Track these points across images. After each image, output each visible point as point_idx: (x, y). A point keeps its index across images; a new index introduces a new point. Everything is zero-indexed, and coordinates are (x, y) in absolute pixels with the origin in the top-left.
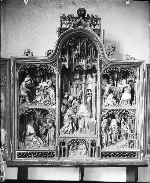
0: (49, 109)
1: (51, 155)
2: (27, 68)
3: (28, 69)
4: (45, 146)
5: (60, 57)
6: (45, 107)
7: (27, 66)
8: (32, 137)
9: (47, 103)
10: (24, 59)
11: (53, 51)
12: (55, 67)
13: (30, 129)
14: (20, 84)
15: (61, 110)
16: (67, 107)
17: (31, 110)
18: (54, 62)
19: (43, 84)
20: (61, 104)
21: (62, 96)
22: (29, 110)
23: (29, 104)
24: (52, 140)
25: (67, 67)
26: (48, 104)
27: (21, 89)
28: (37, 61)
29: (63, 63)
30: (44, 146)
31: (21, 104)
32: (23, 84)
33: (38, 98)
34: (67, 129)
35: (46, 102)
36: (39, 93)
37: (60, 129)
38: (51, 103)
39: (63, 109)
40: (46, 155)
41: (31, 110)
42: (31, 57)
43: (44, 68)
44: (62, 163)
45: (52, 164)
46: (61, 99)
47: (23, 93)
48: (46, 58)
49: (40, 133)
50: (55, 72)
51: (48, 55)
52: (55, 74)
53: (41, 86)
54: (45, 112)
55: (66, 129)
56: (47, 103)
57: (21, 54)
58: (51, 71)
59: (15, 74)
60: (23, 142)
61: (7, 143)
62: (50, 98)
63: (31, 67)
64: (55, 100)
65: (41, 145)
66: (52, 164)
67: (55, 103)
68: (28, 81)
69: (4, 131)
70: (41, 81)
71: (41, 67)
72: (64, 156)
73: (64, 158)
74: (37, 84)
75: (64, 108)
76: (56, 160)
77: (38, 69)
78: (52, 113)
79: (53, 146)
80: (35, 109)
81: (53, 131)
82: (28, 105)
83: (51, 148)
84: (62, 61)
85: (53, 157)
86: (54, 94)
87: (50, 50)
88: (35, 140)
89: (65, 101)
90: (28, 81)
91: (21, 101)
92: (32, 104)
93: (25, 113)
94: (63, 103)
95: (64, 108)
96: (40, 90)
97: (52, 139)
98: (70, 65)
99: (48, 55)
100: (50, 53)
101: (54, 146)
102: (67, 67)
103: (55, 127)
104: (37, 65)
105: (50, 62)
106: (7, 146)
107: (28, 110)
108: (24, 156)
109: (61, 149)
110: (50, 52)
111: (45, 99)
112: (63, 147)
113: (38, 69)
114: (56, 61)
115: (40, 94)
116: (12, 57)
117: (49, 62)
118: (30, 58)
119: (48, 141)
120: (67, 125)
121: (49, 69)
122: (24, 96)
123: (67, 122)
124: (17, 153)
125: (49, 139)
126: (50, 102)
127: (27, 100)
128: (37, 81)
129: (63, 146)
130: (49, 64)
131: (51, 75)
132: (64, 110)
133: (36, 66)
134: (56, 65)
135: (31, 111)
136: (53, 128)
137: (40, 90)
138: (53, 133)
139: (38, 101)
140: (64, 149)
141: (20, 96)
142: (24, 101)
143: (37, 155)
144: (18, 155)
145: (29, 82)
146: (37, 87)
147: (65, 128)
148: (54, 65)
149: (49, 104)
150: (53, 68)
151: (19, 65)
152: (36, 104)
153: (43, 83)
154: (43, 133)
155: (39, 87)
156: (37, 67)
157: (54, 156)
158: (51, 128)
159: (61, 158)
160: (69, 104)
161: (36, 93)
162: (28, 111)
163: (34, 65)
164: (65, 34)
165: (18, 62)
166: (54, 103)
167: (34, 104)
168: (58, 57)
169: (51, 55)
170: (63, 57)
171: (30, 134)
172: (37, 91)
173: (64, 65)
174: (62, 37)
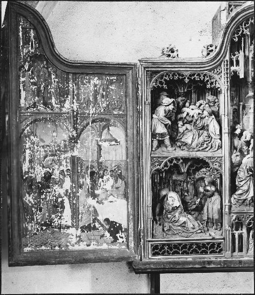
0: (210, 158)
1: (214, 247)
2: (165, 80)
3: (167, 82)
4: (203, 231)
5: (227, 58)
6: (201, 155)
7: (166, 76)
8: (177, 214)
9: (205, 146)
10: (163, 63)
11: (216, 48)
12: (219, 76)
13: (173, 199)
14: (153, 110)
15: (231, 159)
16: (243, 155)
17: (175, 162)
18: (216, 67)
19: (191, 110)
20: (233, 147)
21: (232, 134)
22: (171, 161)
23: (170, 148)
24: (216, 220)
25: (242, 76)
26: (207, 148)
27: (155, 121)
28: (188, 66)
29: (233, 68)
30: (202, 232)
31: (156, 150)
32: (161, 111)
33: (185, 137)
34: (245, 196)
35: (202, 144)
36: (184, 128)
37: (231, 197)
38: (212, 147)
39: (236, 159)
40: (207, 248)
41: (175, 162)
42: (174, 60)
43: (197, 78)
44: (240, 262)
45: (220, 264)
46: (231, 139)
47: (161, 129)
48: (205, 60)
49: (188, 208)
50: (218, 85)
51: (208, 54)
52: (219, 89)
53: (188, 114)
54: (199, 164)
55: (244, 197)
56: (205, 146)
57: (156, 55)
58: (212, 83)
59: (145, 94)
60: (160, 225)
61: (131, 225)
62: (209, 136)
63: (173, 79)
64: (221, 139)
65: (195, 230)
66: (220, 264)
67: (220, 147)
68: (170, 104)
69: (126, 202)
70: (187, 104)
71: (193, 78)
72: (241, 250)
73: (240, 254)
74: (179, 109)
75: (237, 156)
76: (226, 256)
77: (187, 80)
78: (215, 167)
79: (217, 231)
80: (182, 158)
81: (218, 201)
82: (172, 152)
83: (214, 234)
84: (232, 64)
85: (219, 252)
86: (218, 127)
87: (211, 46)
88: (183, 219)
89: (237, 142)
90: (170, 104)
91: (155, 143)
92: (175, 149)
93: (163, 168)
94: (234, 146)
95: (237, 156)
96: (185, 121)
97: (216, 216)
98: (246, 73)
99: (208, 54)
100: (212, 50)
101: (221, 231)
102: (242, 76)
103: (220, 194)
104: (185, 73)
105: (210, 68)
106: (131, 231)
107: (169, 161)
108: (165, 252)
109: (233, 235)
110: (211, 49)
111: (201, 139)
112: (238, 232)
113: (187, 80)
114: (220, 65)
115: (187, 129)
116: (140, 61)
117: (206, 69)
118: (174, 61)
119: (207, 222)
120: (245, 188)
121: (208, 81)
122: (162, 135)
123: (244, 182)
124: (152, 245)
125: (208, 218)
126: (210, 144)
127: (167, 141)
128: (180, 105)
129: (237, 230)
130: (210, 70)
131: (216, 92)
132: (238, 158)
133: (183, 75)
134: (221, 72)
135: (174, 164)
136: (216, 197)
137: (185, 121)
138: (217, 206)
139: (186, 144)
140: (241, 236)
141: (154, 135)
142: (161, 143)
143: (189, 250)
144: (153, 250)
145: (171, 107)
146: (179, 116)
147: (241, 194)
148: (217, 72)
149: (207, 149)
150: (217, 77)
151: (151, 74)
152: (182, 150)
153: (192, 107)
154: (194, 207)
155: (184, 115)
156: (185, 78)
157: (221, 250)
158: (212, 195)
159: (235, 254)
160: (245, 147)
161: (178, 127)
162: (169, 164)
163: (179, 75)
164: (238, 14)
165: (149, 69)
166: (219, 146)
167: (178, 149)
168: (225, 57)
169: (212, 55)
170: (233, 57)
171: (175, 209)
172: (180, 123)
173: (235, 72)
174: (233, 19)
